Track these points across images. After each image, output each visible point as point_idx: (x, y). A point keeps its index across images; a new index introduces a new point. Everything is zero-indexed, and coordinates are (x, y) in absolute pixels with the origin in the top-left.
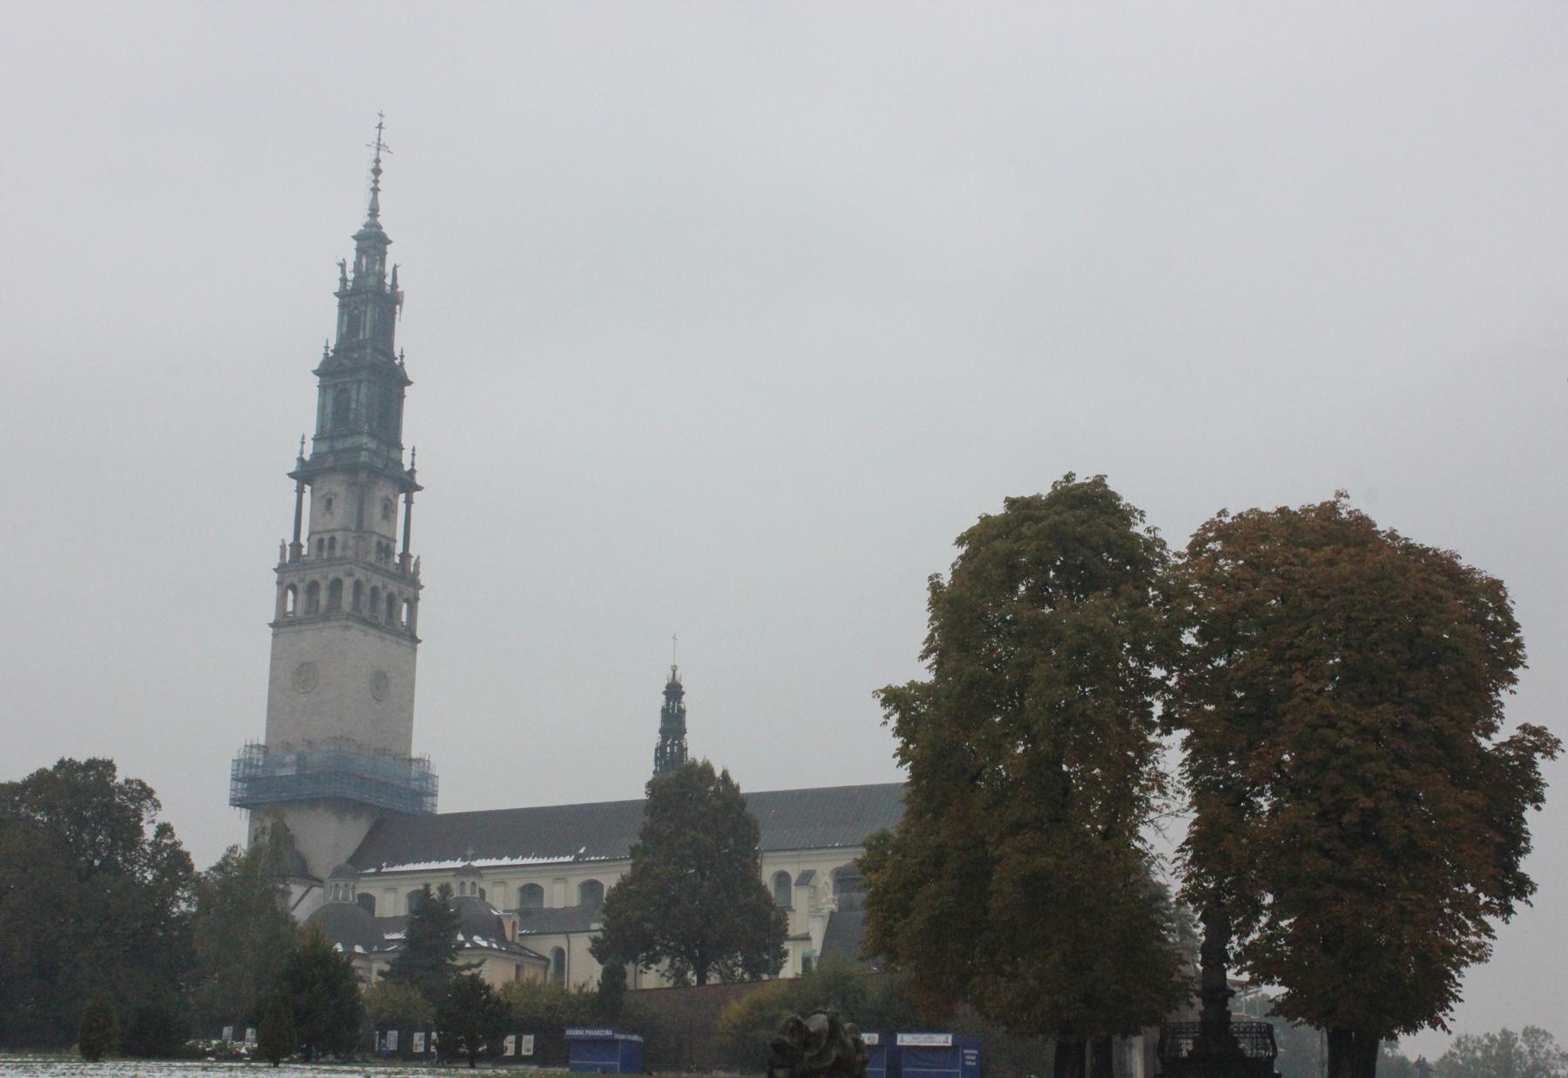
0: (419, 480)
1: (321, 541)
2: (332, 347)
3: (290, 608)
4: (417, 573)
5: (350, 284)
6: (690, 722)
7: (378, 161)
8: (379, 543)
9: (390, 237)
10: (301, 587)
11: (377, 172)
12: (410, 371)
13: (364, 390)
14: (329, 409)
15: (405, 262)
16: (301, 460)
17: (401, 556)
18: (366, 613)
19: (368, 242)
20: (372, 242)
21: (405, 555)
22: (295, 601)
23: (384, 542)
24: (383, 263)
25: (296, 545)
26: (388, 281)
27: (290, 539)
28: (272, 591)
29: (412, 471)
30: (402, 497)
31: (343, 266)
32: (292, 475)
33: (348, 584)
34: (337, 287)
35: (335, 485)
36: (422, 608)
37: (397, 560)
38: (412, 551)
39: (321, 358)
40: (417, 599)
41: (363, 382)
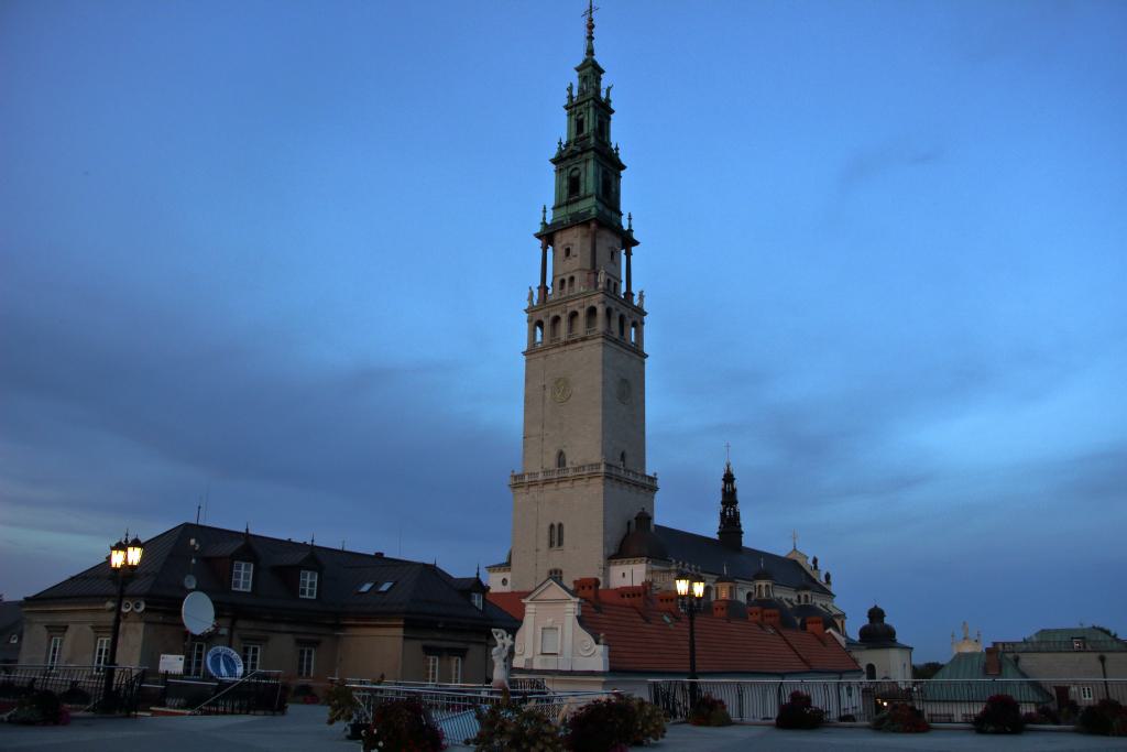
0: (635, 236)
1: (563, 281)
2: (564, 143)
3: (539, 339)
9: (603, 67)
11: (591, 27)
12: (623, 158)
14: (565, 183)
15: (613, 83)
16: (544, 223)
19: (589, 69)
20: (591, 71)
21: (629, 294)
22: (542, 336)
23: (613, 281)
25: (543, 288)
26: (603, 95)
29: (630, 230)
30: (623, 251)
32: (539, 236)
34: (566, 102)
35: (575, 238)
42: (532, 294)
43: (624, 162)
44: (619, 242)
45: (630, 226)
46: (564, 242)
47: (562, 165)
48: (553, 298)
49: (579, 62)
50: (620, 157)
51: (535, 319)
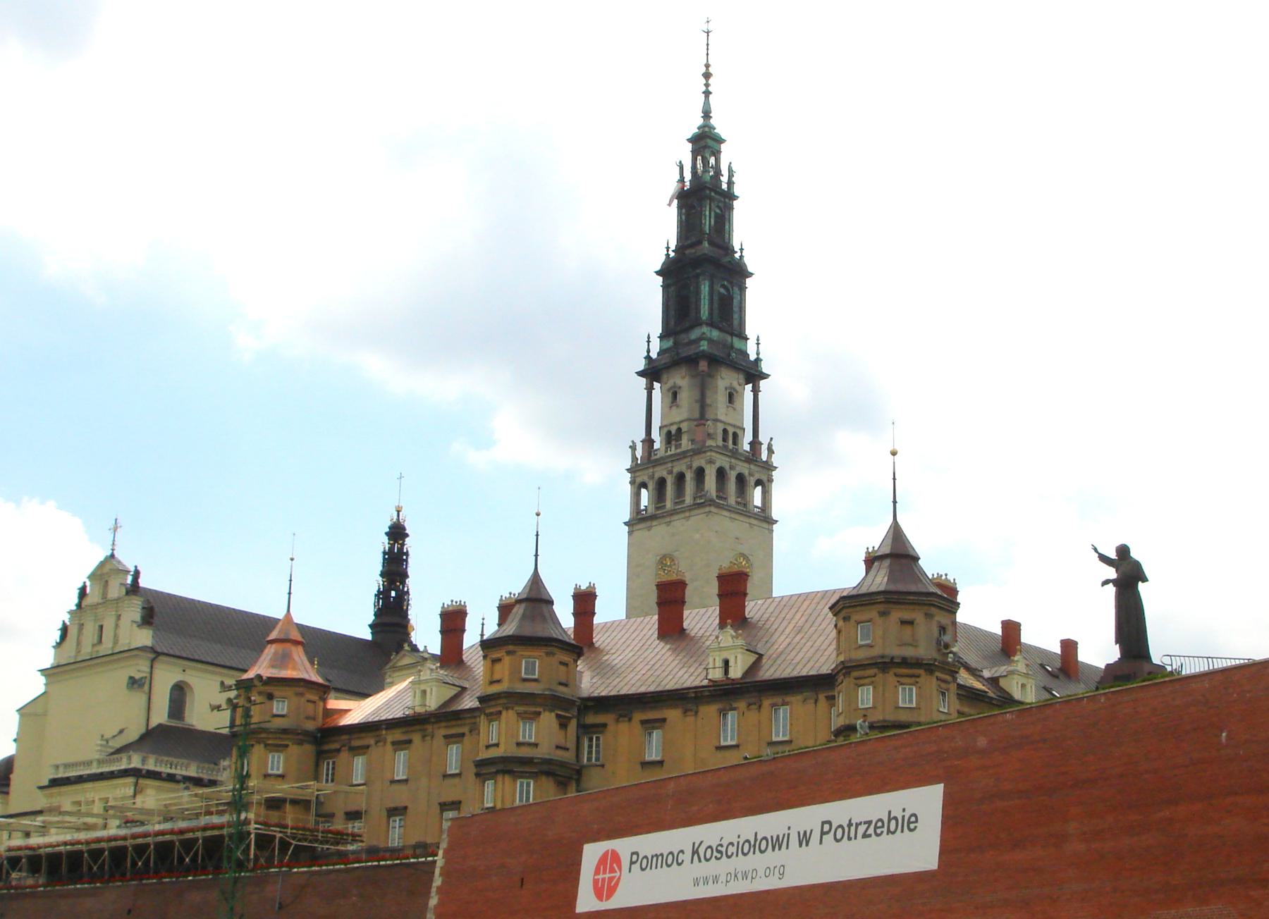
0: (765, 368)
1: (669, 433)
2: (673, 247)
5: (688, 184)
7: (707, 66)
11: (707, 76)
12: (750, 264)
16: (648, 358)
20: (705, 142)
21: (755, 443)
23: (731, 430)
24: (718, 161)
25: (648, 441)
26: (724, 179)
27: (642, 435)
28: (627, 489)
29: (758, 360)
30: (749, 387)
32: (641, 374)
35: (680, 379)
37: (747, 447)
38: (763, 438)
39: (663, 258)
41: (704, 275)
42: (633, 448)
43: (750, 270)
44: (742, 377)
45: (758, 354)
46: (670, 383)
48: (661, 454)
49: (694, 130)
50: (746, 260)
51: (639, 480)
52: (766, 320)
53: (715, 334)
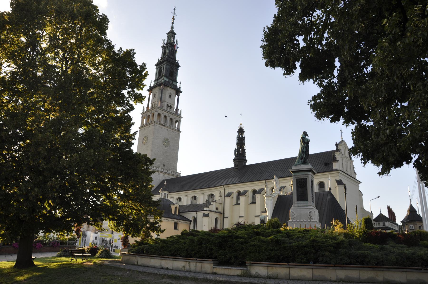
0: (181, 90)
4: (181, 114)
6: (246, 142)
7: (174, 17)
8: (167, 105)
10: (146, 117)
11: (173, 19)
13: (165, 66)
16: (150, 86)
17: (176, 109)
18: (162, 123)
19: (170, 34)
20: (172, 34)
21: (177, 109)
23: (169, 105)
27: (147, 106)
28: (141, 119)
29: (180, 88)
31: (164, 40)
33: (156, 114)
36: (182, 123)
37: (175, 110)
40: (180, 121)
44: (174, 91)
47: (158, 67)
49: (168, 31)
50: (179, 63)
52: (182, 78)
53: (167, 80)
